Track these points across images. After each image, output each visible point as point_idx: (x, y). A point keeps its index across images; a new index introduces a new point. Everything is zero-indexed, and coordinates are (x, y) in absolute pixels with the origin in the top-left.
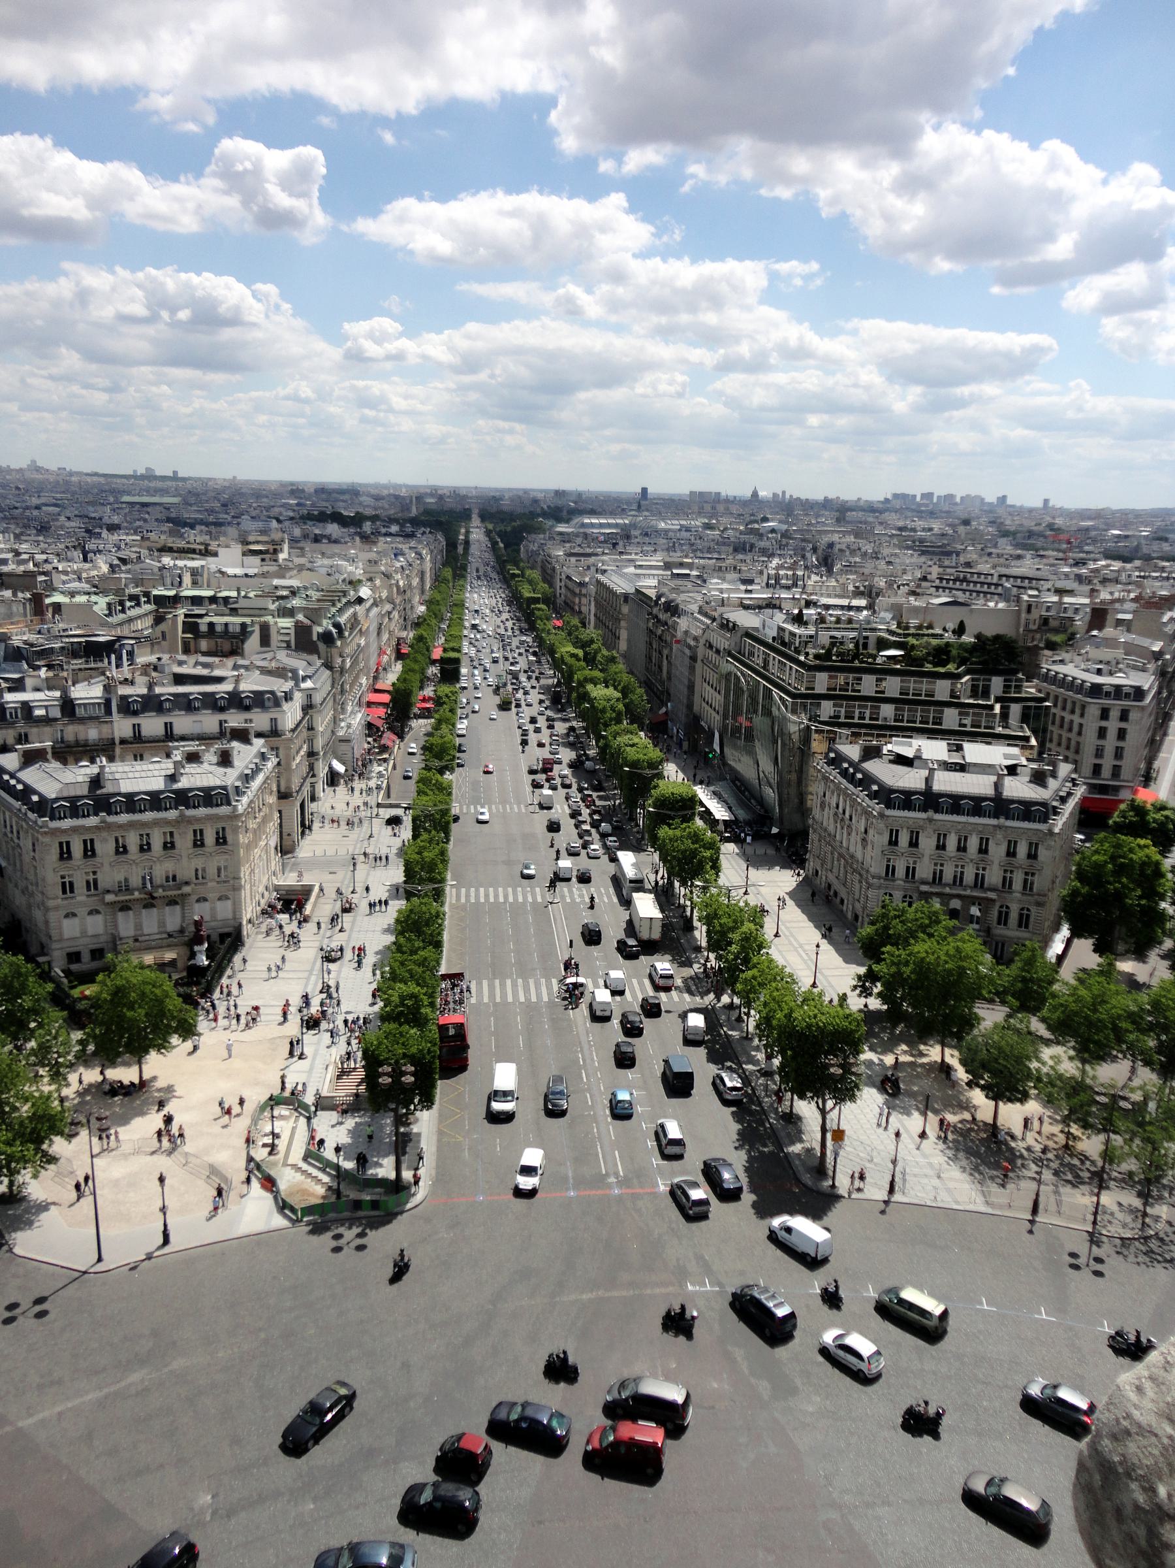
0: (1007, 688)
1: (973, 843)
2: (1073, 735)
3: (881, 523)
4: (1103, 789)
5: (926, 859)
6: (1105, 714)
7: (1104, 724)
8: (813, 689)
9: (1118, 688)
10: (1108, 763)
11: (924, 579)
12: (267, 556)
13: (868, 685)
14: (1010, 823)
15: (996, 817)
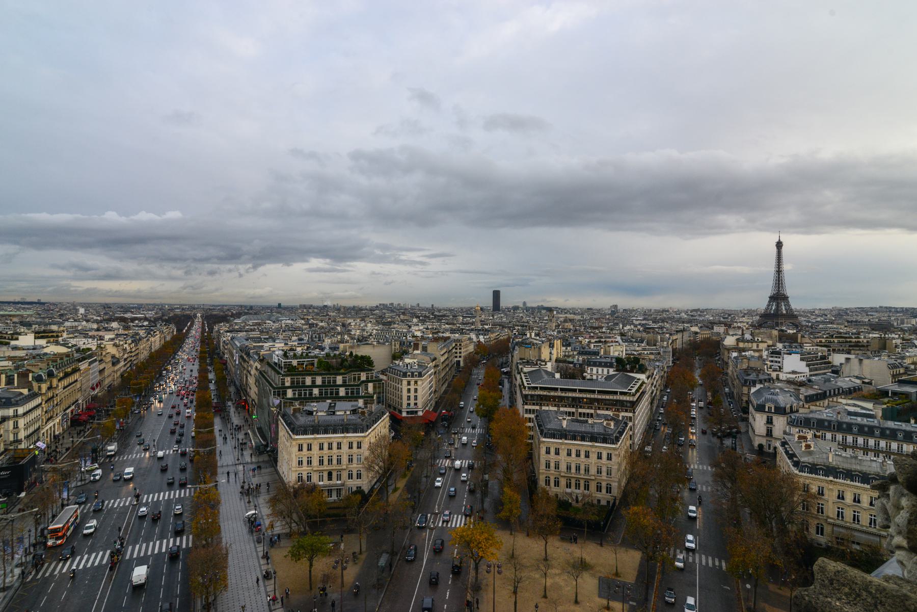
0: (367, 378)
1: (335, 446)
2: (399, 393)
3: (372, 315)
4: (412, 412)
5: (315, 455)
6: (409, 384)
7: (409, 387)
8: (284, 384)
9: (413, 373)
10: (412, 402)
11: (371, 335)
12: (52, 340)
13: (308, 381)
14: (348, 435)
15: (343, 433)
